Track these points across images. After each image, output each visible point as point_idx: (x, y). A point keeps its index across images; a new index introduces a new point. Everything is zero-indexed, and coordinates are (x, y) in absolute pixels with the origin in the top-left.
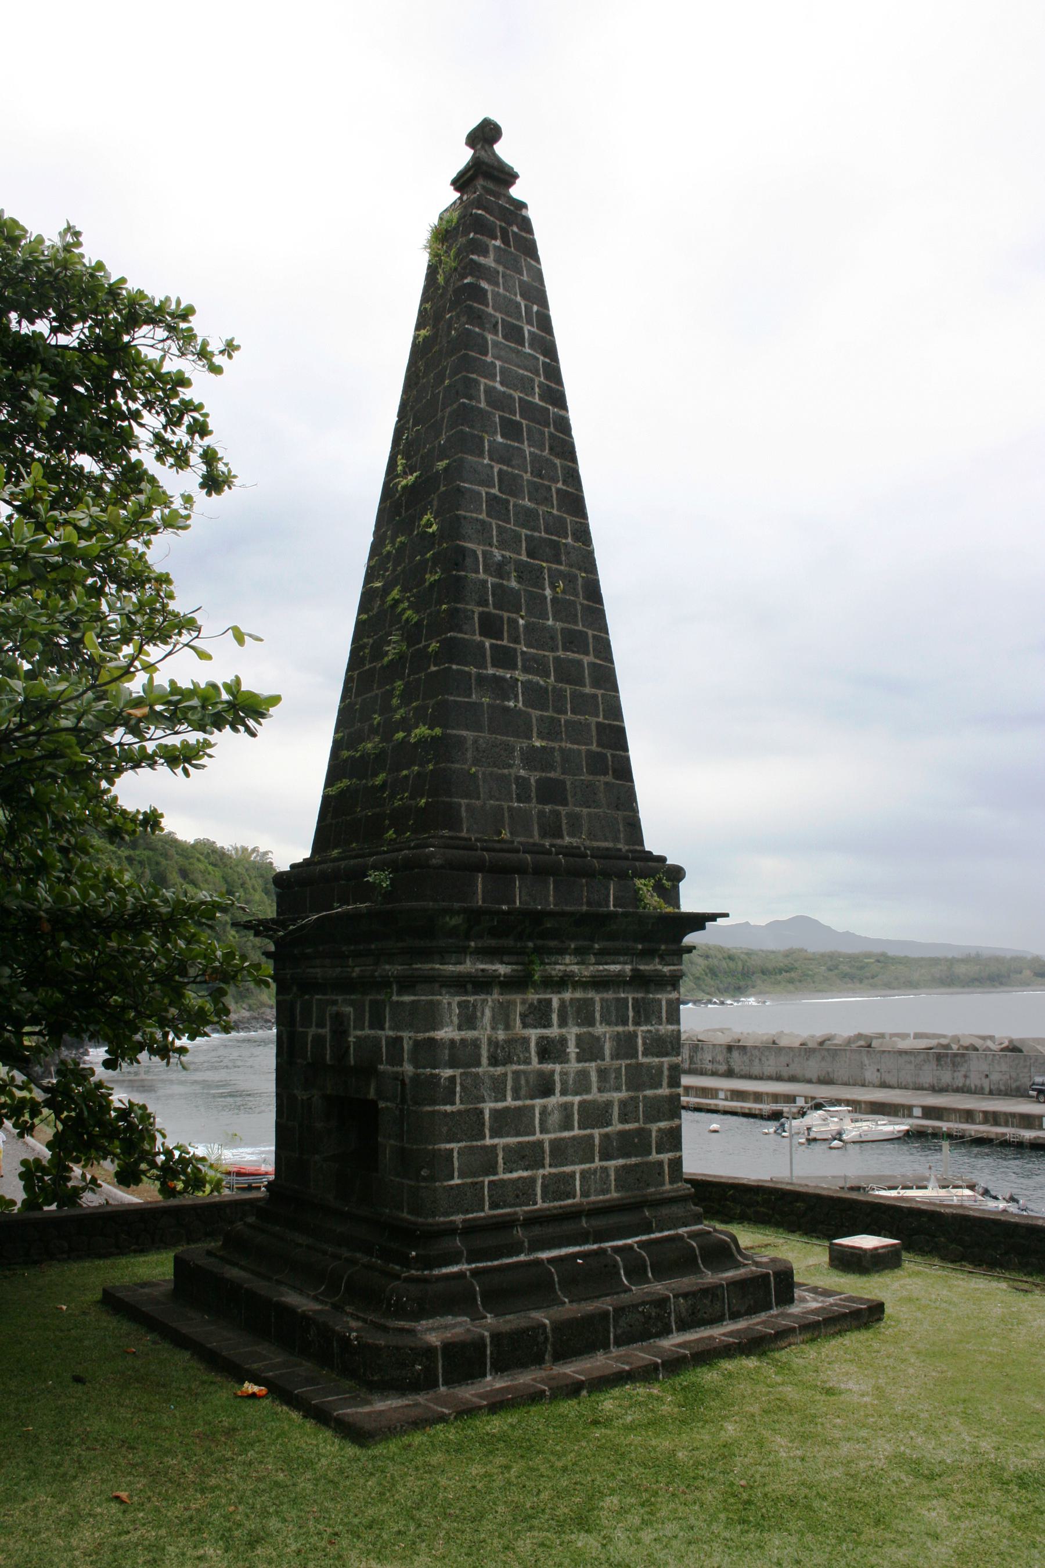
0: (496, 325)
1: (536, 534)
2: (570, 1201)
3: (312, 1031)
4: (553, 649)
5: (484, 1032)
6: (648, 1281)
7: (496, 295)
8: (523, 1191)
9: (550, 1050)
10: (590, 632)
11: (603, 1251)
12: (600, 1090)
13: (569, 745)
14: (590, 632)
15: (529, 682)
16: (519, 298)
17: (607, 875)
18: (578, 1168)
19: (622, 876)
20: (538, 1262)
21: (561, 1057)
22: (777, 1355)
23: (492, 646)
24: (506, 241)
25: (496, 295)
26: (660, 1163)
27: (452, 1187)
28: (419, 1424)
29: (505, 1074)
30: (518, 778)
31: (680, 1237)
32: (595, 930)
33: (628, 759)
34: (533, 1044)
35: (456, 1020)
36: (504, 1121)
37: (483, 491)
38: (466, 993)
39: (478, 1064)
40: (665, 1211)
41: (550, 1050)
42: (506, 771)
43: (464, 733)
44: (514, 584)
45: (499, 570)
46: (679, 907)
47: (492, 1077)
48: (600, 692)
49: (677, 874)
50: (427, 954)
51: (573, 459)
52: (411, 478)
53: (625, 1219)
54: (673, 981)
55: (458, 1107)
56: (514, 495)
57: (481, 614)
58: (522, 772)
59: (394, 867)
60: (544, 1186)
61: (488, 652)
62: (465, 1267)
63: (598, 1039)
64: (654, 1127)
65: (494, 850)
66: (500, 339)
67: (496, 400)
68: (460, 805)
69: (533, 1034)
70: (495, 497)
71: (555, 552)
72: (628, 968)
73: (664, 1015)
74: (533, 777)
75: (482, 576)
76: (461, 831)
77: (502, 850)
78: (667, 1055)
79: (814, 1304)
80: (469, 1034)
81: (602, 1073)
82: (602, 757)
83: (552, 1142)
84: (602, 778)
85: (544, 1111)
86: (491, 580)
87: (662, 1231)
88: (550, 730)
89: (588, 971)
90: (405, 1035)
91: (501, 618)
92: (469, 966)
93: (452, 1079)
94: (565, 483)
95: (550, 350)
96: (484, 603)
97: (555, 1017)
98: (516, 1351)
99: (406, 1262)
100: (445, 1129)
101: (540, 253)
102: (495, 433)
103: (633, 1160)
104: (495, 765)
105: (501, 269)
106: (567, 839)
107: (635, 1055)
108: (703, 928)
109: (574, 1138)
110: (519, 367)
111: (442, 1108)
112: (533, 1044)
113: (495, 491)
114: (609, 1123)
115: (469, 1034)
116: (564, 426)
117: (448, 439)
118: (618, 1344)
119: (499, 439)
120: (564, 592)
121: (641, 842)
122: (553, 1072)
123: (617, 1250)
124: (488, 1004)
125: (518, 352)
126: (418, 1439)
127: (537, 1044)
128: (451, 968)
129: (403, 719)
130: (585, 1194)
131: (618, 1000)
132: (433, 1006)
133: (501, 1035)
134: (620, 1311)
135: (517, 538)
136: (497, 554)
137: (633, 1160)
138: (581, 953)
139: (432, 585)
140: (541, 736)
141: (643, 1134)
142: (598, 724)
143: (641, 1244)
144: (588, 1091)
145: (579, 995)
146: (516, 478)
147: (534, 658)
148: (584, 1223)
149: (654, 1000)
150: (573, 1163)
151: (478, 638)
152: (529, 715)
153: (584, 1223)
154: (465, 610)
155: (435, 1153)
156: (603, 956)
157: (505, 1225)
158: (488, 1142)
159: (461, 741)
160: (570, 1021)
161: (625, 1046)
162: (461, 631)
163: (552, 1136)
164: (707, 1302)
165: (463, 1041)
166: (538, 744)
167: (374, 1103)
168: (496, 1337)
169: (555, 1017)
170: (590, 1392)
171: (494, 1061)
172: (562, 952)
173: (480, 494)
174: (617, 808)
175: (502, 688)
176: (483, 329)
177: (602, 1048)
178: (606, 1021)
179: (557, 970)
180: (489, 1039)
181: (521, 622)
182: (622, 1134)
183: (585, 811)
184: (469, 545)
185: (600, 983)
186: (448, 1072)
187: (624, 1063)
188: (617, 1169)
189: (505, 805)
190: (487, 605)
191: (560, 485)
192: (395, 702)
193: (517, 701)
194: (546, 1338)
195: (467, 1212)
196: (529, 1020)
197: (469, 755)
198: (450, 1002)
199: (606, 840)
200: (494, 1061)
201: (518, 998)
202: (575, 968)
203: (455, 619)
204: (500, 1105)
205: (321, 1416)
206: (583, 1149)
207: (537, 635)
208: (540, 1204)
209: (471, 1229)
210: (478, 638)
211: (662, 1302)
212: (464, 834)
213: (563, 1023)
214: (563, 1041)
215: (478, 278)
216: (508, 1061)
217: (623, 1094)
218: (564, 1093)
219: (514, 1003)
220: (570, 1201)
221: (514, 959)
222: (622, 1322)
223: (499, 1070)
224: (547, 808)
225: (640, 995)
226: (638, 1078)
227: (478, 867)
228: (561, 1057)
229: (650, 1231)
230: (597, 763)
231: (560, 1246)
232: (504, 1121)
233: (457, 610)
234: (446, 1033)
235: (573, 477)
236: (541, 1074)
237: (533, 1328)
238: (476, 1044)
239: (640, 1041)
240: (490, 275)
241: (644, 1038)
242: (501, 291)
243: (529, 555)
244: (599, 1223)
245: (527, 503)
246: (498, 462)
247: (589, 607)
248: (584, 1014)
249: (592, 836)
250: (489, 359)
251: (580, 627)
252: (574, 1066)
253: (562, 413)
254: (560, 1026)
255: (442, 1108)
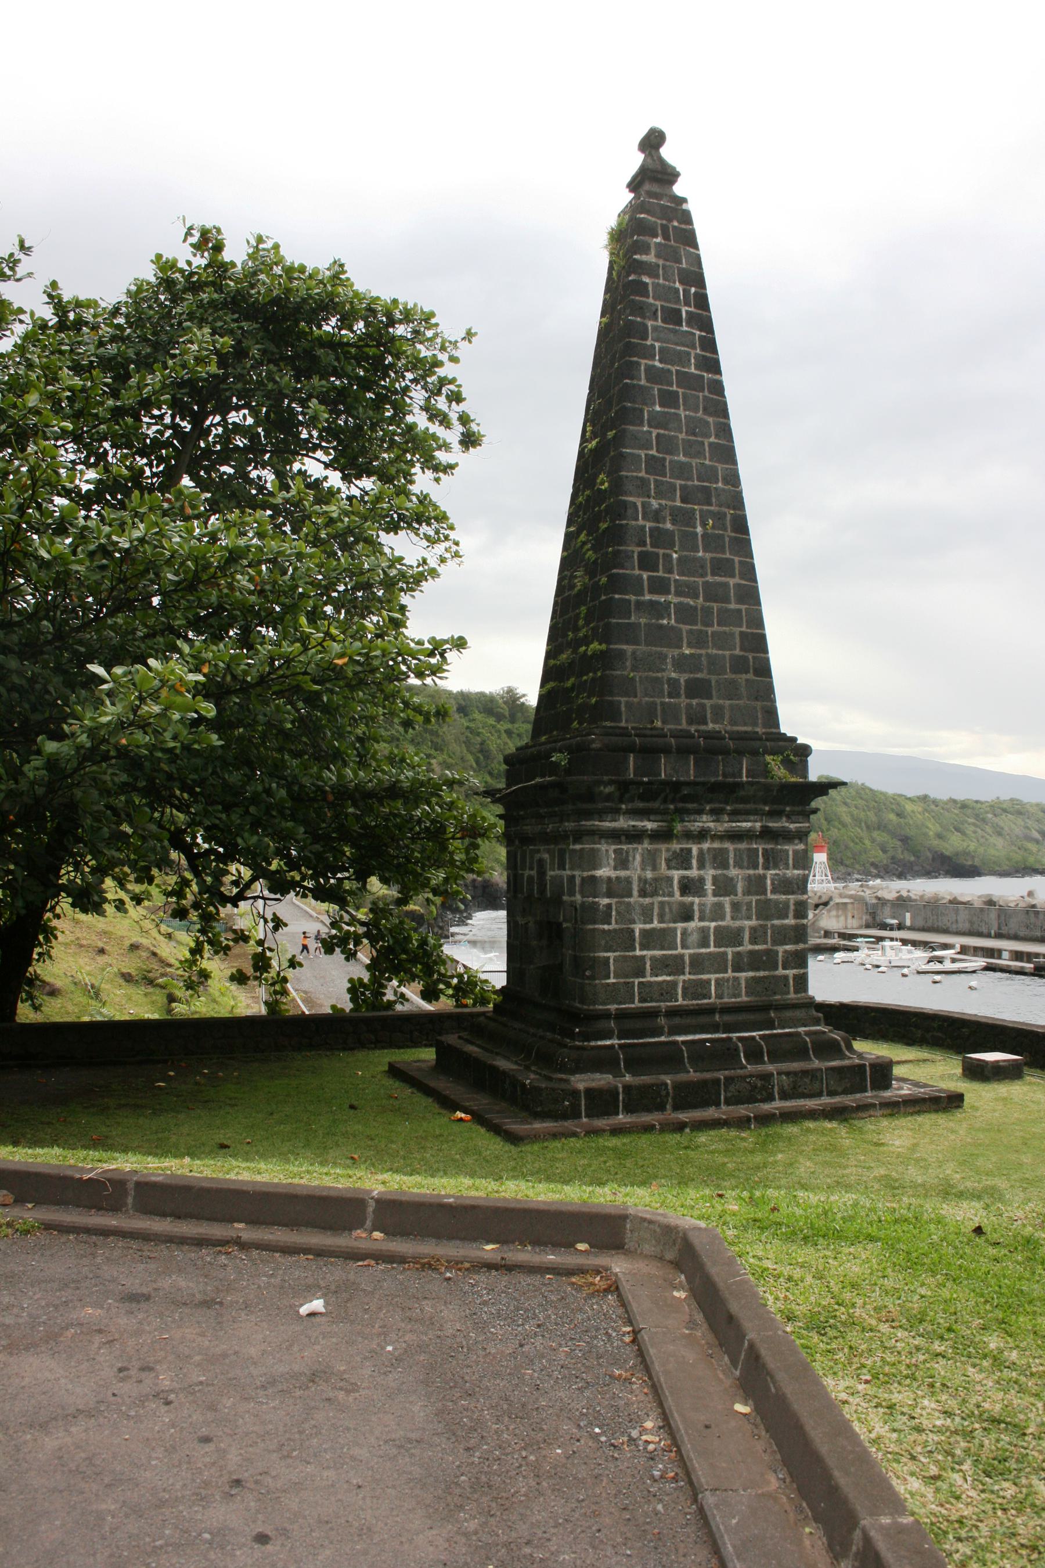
0: (655, 313)
1: (690, 483)
2: (706, 1001)
3: (527, 873)
4: (702, 576)
5: (636, 872)
6: (764, 1063)
7: (656, 286)
8: (667, 992)
9: (688, 887)
10: (736, 559)
11: (730, 1039)
12: (733, 918)
13: (715, 651)
14: (736, 559)
15: (680, 603)
16: (677, 285)
17: (740, 753)
18: (713, 977)
19: (754, 753)
20: (675, 1043)
21: (700, 892)
22: (856, 1122)
23: (649, 578)
24: (666, 237)
25: (656, 286)
26: (786, 977)
27: (608, 985)
28: (555, 1136)
29: (652, 904)
30: (669, 679)
31: (798, 1034)
32: (724, 795)
33: (768, 660)
34: (676, 882)
35: (612, 863)
36: (650, 939)
37: (642, 453)
38: (620, 843)
39: (630, 895)
40: (788, 1014)
41: (688, 887)
42: (659, 675)
43: (624, 647)
44: (669, 526)
45: (657, 516)
46: (806, 776)
47: (641, 905)
48: (743, 607)
49: (804, 751)
50: (589, 815)
51: (725, 414)
52: (594, 443)
53: (751, 1017)
54: (801, 836)
55: (613, 926)
56: (671, 453)
57: (640, 554)
58: (673, 675)
59: (570, 750)
60: (684, 989)
61: (646, 583)
62: (616, 1041)
63: (732, 879)
64: (781, 949)
65: (645, 736)
66: (660, 323)
67: (654, 375)
68: (620, 702)
69: (676, 874)
70: (653, 456)
71: (706, 496)
72: (758, 825)
73: (791, 862)
74: (683, 678)
75: (641, 522)
76: (620, 721)
77: (652, 736)
78: (793, 893)
79: (906, 1091)
80: (623, 873)
81: (735, 906)
82: (745, 659)
83: (690, 955)
84: (744, 676)
85: (684, 933)
86: (648, 525)
87: (784, 1028)
88: (698, 640)
89: (725, 825)
90: (577, 873)
91: (657, 554)
92: (623, 823)
93: (609, 906)
94: (717, 436)
95: (706, 324)
96: (643, 543)
97: (694, 862)
98: (642, 1100)
99: (572, 1036)
100: (603, 942)
101: (699, 240)
102: (654, 404)
103: (762, 974)
104: (650, 670)
105: (661, 262)
106: (711, 726)
107: (765, 893)
108: (826, 794)
109: (710, 954)
110: (677, 344)
111: (601, 926)
112: (676, 882)
113: (653, 452)
114: (741, 944)
115: (623, 873)
116: (718, 388)
117: (616, 413)
118: (728, 1103)
119: (658, 408)
120: (713, 527)
121: (777, 725)
122: (692, 904)
123: (740, 1039)
124: (638, 852)
125: (675, 332)
126: (557, 1144)
127: (679, 882)
128: (607, 824)
129: (586, 636)
130: (719, 996)
131: (749, 850)
132: (594, 852)
133: (649, 874)
134: (729, 1080)
135: (673, 488)
136: (655, 504)
137: (762, 974)
138: (717, 813)
139: (604, 531)
140: (690, 645)
141: (771, 954)
142: (741, 633)
143: (762, 1037)
144: (723, 918)
145: (716, 845)
146: (671, 438)
147: (687, 585)
148: (717, 1017)
149: (781, 851)
150: (709, 972)
151: (637, 572)
152: (680, 630)
153: (717, 1017)
154: (626, 551)
155: (595, 960)
156: (735, 815)
157: (654, 1014)
158: (638, 953)
159: (621, 654)
160: (707, 865)
161: (756, 885)
162: (623, 568)
163: (691, 951)
164: (807, 1080)
165: (617, 878)
166: (687, 652)
167: (561, 924)
168: (627, 1088)
169: (694, 862)
170: (692, 1130)
171: (643, 893)
172: (700, 812)
173: (639, 456)
174: (757, 699)
175: (657, 610)
176: (644, 317)
177: (735, 887)
178: (738, 865)
179: (696, 826)
180: (640, 879)
181: (675, 556)
182: (751, 953)
183: (728, 702)
184: (631, 499)
185: (735, 836)
186: (606, 901)
187: (754, 898)
188: (747, 980)
189: (658, 700)
190: (644, 544)
191: (712, 439)
192: (581, 622)
193: (670, 619)
194: (668, 1094)
195: (621, 1003)
196: (673, 864)
197: (628, 664)
198: (608, 850)
199: (745, 724)
200: (643, 893)
201: (663, 847)
202: (712, 825)
203: (618, 559)
204: (648, 926)
205: (496, 1130)
206: (718, 963)
207: (688, 566)
208: (680, 1001)
209: (622, 1016)
210: (637, 572)
211: (767, 1077)
212: (623, 724)
213: (701, 866)
214: (701, 880)
215: (640, 274)
216: (654, 893)
217: (754, 922)
218: (701, 919)
219: (660, 851)
220: (706, 1001)
221: (659, 817)
222: (732, 1088)
223: (647, 900)
224: (694, 702)
225: (769, 846)
226: (766, 910)
227: (631, 749)
228: (700, 892)
229: (772, 1027)
230: (739, 665)
231: (694, 1033)
232: (650, 939)
233: (619, 551)
234: (604, 872)
235: (725, 431)
236: (682, 905)
237: (657, 1085)
238: (628, 881)
239: (769, 882)
240: (651, 270)
241: (772, 880)
242: (661, 281)
243: (683, 501)
244: (727, 1018)
245: (682, 458)
246: (656, 428)
247: (736, 538)
248: (720, 860)
249: (732, 722)
250: (649, 343)
251: (728, 556)
252: (710, 899)
253: (717, 377)
254: (699, 869)
255: (601, 926)
